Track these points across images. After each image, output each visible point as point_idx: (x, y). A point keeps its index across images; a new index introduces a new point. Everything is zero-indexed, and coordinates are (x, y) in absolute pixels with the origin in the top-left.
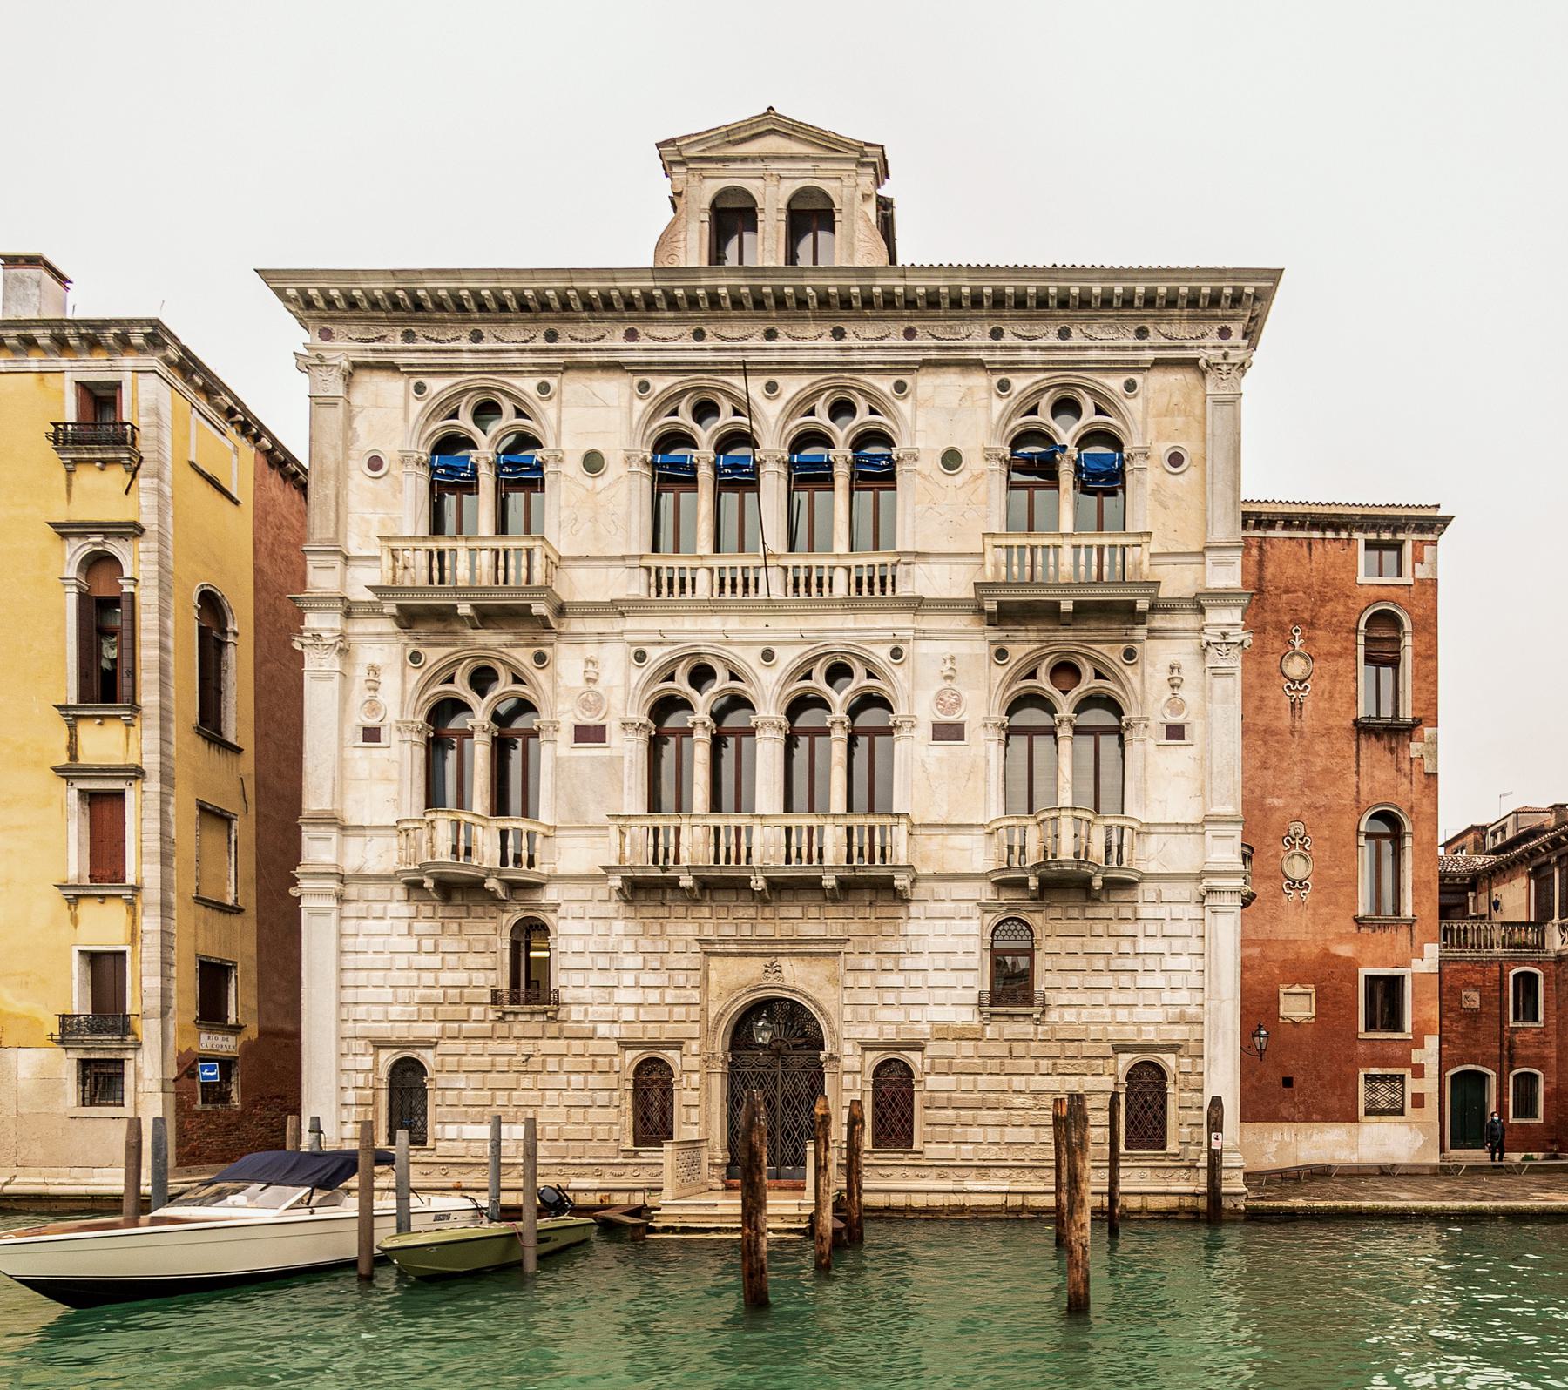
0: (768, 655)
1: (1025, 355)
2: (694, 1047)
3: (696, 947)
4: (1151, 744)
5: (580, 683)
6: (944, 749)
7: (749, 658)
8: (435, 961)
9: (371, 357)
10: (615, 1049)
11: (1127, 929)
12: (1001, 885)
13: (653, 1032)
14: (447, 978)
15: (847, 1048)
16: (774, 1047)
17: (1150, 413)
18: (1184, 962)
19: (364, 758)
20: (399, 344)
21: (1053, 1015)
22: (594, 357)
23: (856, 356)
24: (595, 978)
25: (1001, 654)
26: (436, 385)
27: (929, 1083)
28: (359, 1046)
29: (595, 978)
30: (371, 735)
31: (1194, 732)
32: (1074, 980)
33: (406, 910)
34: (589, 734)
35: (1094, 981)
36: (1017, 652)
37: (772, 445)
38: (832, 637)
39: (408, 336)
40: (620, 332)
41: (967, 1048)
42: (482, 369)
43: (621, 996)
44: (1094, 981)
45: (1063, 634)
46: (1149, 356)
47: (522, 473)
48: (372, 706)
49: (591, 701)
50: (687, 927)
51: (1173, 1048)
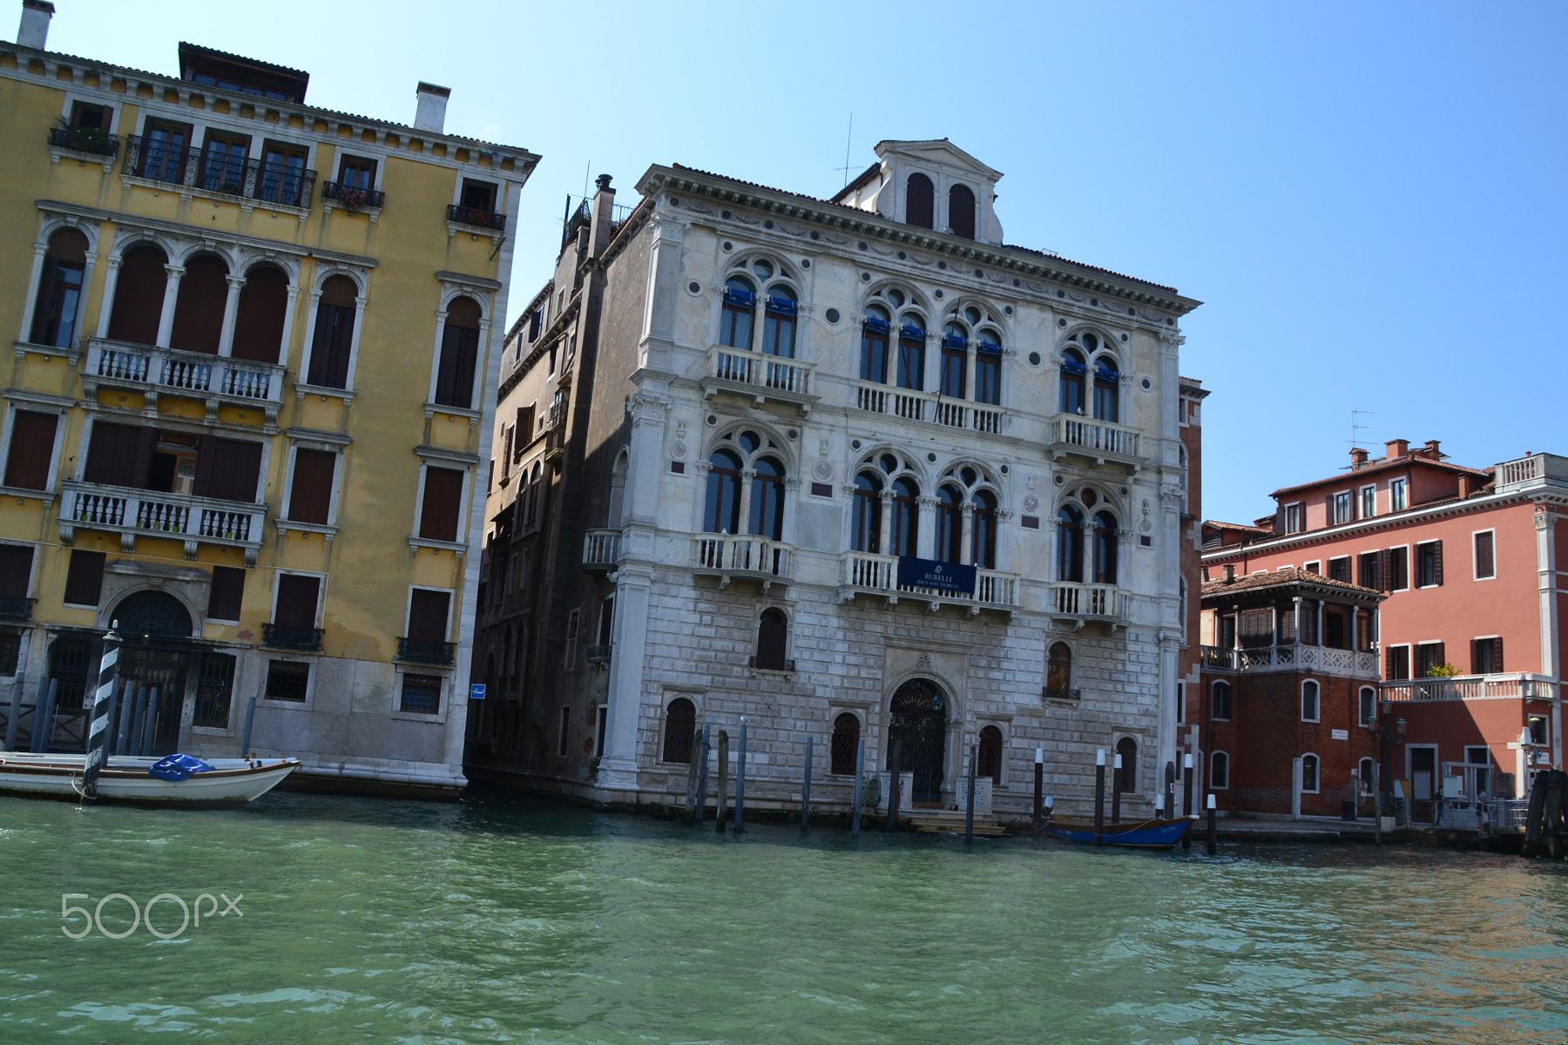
0: (932, 457)
1: (1076, 310)
2: (877, 708)
3: (882, 641)
4: (1133, 547)
5: (817, 455)
6: (1027, 532)
7: (920, 457)
8: (711, 632)
9: (702, 222)
10: (826, 704)
11: (1121, 656)
12: (1056, 621)
13: (851, 696)
14: (718, 644)
15: (969, 717)
17: (1133, 355)
18: (1147, 679)
20: (720, 219)
21: (1082, 705)
22: (840, 254)
23: (988, 289)
24: (817, 656)
25: (1059, 480)
26: (738, 247)
28: (654, 688)
29: (817, 656)
30: (678, 467)
31: (1156, 540)
32: (1093, 685)
33: (693, 594)
34: (821, 490)
35: (1103, 686)
36: (1067, 479)
37: (936, 329)
38: (969, 453)
39: (726, 215)
40: (856, 244)
41: (1035, 723)
42: (769, 244)
43: (834, 670)
44: (1103, 686)
45: (1091, 474)
46: (1135, 325)
47: (785, 310)
48: (681, 450)
49: (826, 469)
50: (876, 627)
51: (1142, 731)
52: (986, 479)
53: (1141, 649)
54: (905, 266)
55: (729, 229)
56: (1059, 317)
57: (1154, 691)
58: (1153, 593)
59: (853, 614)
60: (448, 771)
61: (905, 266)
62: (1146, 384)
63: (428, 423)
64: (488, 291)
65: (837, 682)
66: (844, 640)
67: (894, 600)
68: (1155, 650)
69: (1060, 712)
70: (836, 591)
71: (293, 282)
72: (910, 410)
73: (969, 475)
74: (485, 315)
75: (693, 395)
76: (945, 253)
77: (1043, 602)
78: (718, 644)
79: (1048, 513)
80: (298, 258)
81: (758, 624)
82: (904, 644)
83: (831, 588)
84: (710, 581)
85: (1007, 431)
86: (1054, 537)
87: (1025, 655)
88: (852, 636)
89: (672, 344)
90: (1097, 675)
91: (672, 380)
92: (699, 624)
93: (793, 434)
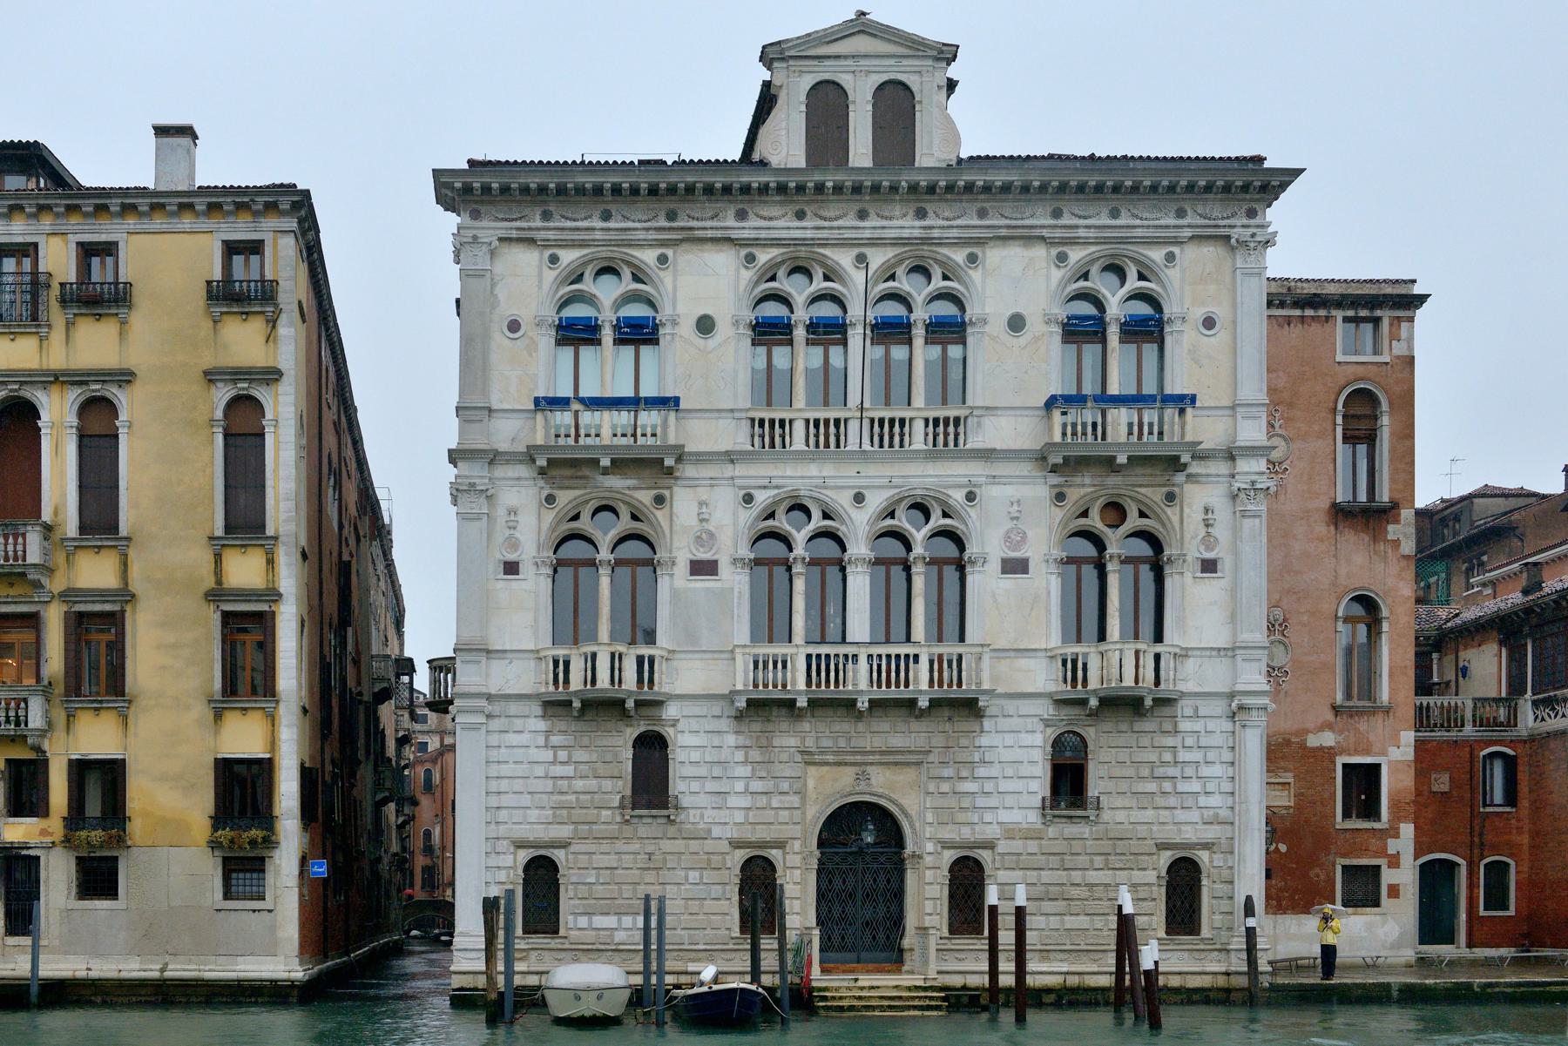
0: (859, 498)
2: (797, 845)
3: (798, 758)
5: (694, 522)
6: (1012, 582)
8: (569, 770)
9: (514, 234)
11: (1169, 741)
12: (1061, 703)
13: (762, 834)
14: (579, 784)
15: (930, 847)
16: (862, 844)
18: (1217, 770)
20: (539, 223)
22: (710, 234)
23: (936, 233)
24: (710, 786)
26: (568, 257)
28: (503, 845)
29: (710, 786)
30: (511, 568)
31: (1226, 566)
33: (542, 725)
38: (915, 482)
39: (546, 216)
40: (731, 213)
41: (1033, 846)
42: (608, 243)
46: (1188, 233)
48: (513, 544)
49: (705, 538)
50: (789, 738)
51: (1206, 846)
52: (945, 515)
53: (1202, 727)
54: (805, 229)
55: (551, 235)
56: (1054, 251)
57: (1227, 787)
58: (1222, 641)
59: (756, 727)
60: (284, 962)
61: (805, 229)
62: (1209, 323)
63: (218, 559)
64: (268, 382)
65: (739, 817)
66: (746, 762)
67: (802, 702)
68: (1228, 726)
69: (1071, 830)
70: (731, 697)
71: (45, 417)
73: (921, 508)
74: (269, 415)
75: (523, 471)
76: (866, 193)
77: (1043, 677)
78: (579, 784)
80: (45, 385)
81: (629, 754)
82: (830, 758)
83: (723, 697)
85: (976, 440)
86: (1055, 584)
87: (1016, 754)
88: (755, 755)
89: (490, 410)
90: (1131, 772)
91: (494, 458)
92: (554, 763)
93: (659, 500)
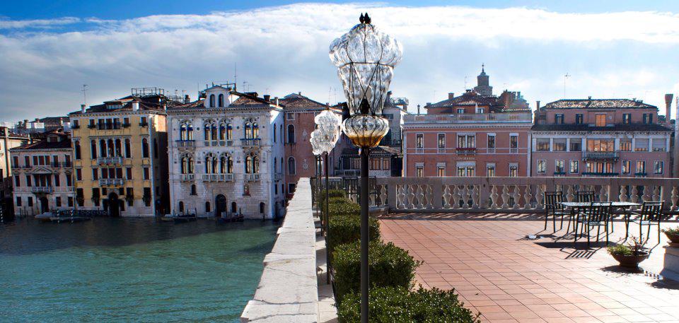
16: (221, 200)
19: (174, 165)
27: (238, 206)
30: (176, 163)
49: (199, 159)
54: (209, 116)
72: (214, 144)
76: (218, 111)
79: (242, 159)
84: (184, 182)
87: (239, 188)
